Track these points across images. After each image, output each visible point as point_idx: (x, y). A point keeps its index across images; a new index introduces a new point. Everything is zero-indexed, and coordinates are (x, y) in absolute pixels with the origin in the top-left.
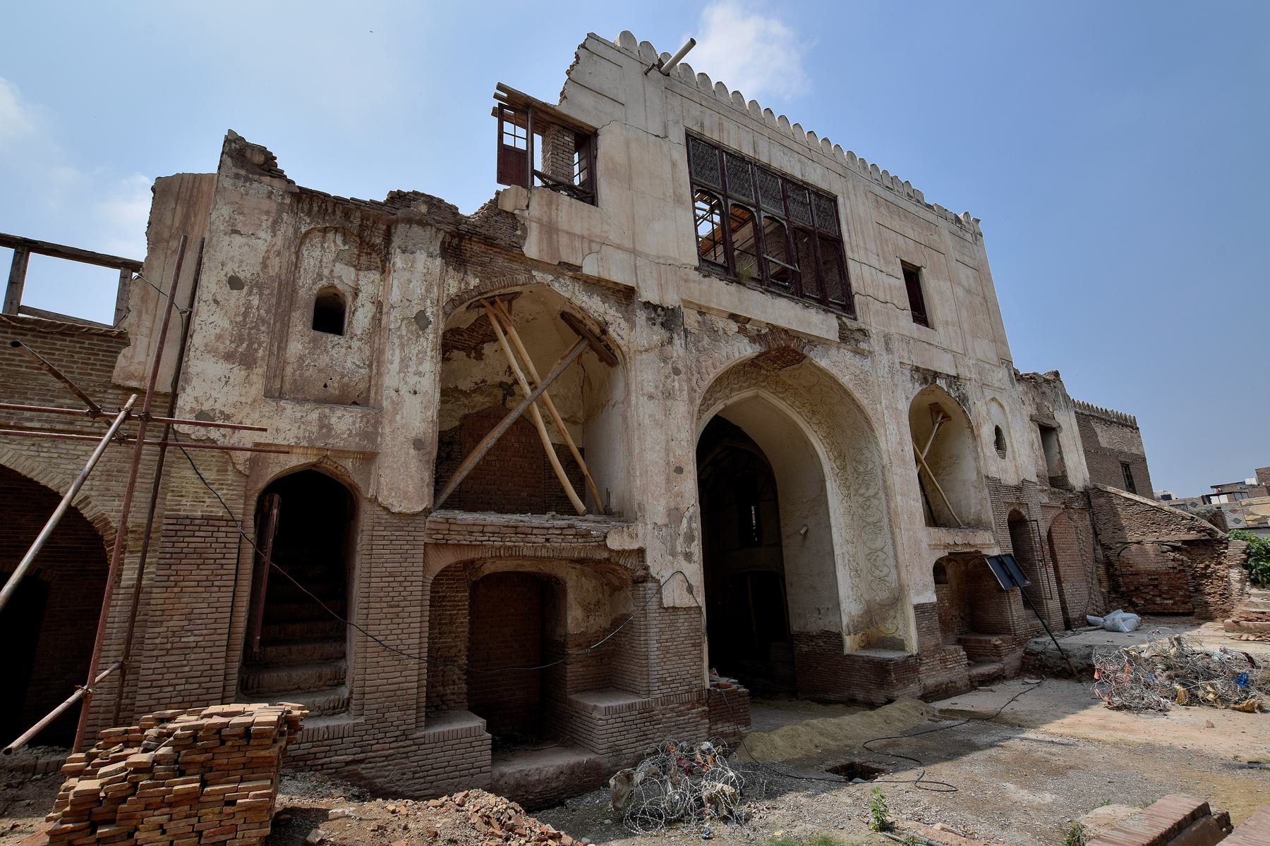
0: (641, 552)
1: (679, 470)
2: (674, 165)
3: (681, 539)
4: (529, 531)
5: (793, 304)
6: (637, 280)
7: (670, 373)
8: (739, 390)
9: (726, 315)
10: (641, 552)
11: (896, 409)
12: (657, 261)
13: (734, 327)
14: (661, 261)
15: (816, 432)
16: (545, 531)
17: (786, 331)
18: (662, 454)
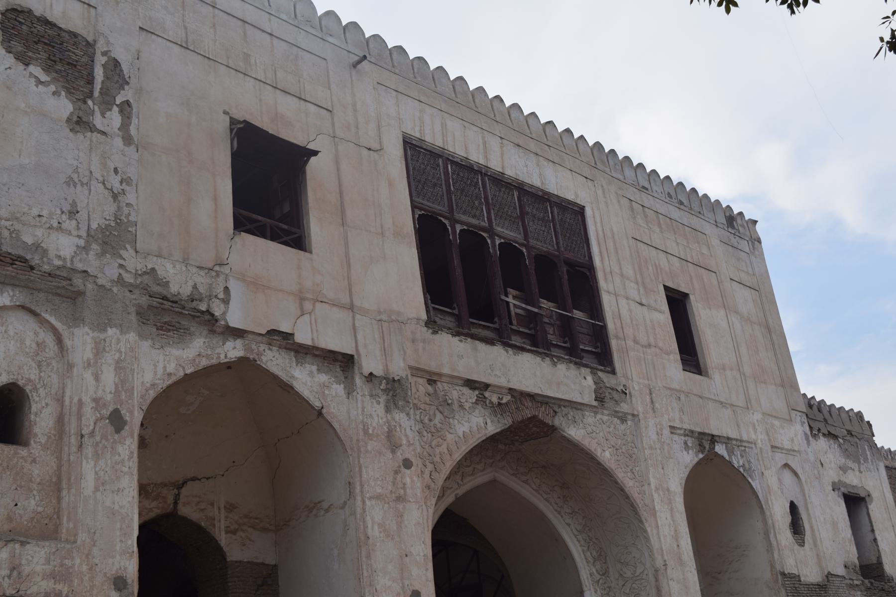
2: (391, 185)
5: (538, 359)
6: (357, 346)
7: (399, 467)
8: (472, 475)
9: (460, 382)
11: (668, 490)
12: (379, 318)
13: (469, 396)
14: (384, 317)
15: (569, 525)
17: (532, 397)
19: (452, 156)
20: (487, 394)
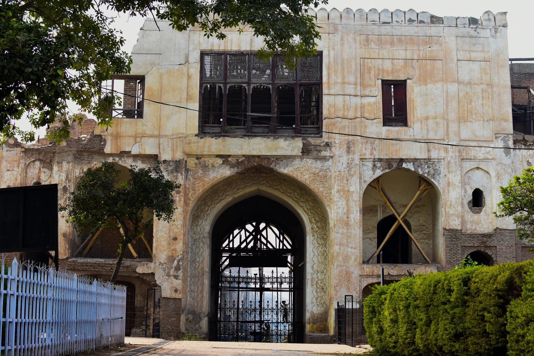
0: (153, 274)
1: (175, 239)
2: (189, 77)
3: (173, 269)
4: (104, 265)
5: (265, 139)
10: (153, 274)
11: (348, 191)
12: (172, 137)
13: (220, 161)
14: (175, 137)
15: (302, 207)
16: (110, 265)
17: (259, 156)
18: (167, 232)
19: (230, 52)
20: (230, 159)
